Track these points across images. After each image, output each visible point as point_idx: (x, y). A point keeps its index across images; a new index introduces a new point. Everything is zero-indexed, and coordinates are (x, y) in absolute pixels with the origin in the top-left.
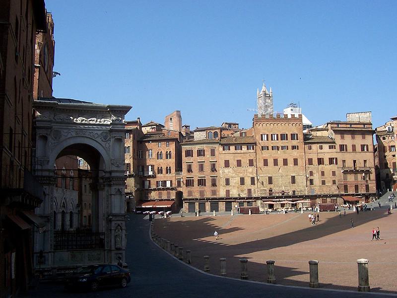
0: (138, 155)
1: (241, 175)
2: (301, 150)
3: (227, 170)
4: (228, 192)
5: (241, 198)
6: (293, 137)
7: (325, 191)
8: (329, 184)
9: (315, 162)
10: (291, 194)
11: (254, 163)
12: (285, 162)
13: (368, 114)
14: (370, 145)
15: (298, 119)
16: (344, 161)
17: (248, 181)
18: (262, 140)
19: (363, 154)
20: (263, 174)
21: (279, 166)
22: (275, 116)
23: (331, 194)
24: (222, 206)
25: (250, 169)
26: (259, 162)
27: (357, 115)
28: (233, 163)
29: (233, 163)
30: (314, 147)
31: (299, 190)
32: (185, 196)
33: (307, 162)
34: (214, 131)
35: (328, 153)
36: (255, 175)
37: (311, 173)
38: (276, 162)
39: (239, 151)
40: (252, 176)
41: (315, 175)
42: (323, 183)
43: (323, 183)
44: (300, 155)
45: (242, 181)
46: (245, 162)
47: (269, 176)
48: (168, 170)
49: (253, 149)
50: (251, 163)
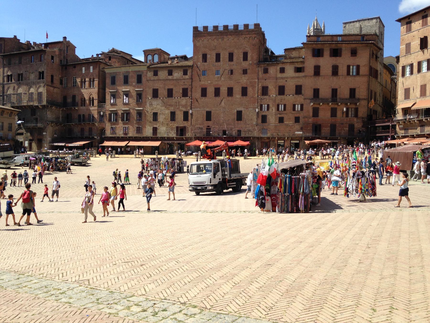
0: (61, 83)
1: (172, 109)
4: (155, 130)
7: (283, 131)
8: (289, 121)
10: (234, 133)
11: (189, 93)
12: (230, 92)
13: (374, 21)
14: (364, 66)
16: (316, 92)
19: (349, 79)
20: (200, 108)
22: (221, 29)
23: (291, 135)
25: (184, 101)
27: (357, 25)
28: (163, 92)
29: (163, 92)
30: (273, 70)
31: (246, 130)
32: (108, 133)
33: (260, 91)
35: (292, 78)
36: (189, 108)
38: (217, 92)
39: (170, 77)
40: (184, 110)
41: (270, 110)
42: (281, 120)
43: (281, 120)
44: (251, 82)
45: (173, 115)
46: (178, 91)
47: (208, 110)
48: (92, 100)
50: (185, 93)
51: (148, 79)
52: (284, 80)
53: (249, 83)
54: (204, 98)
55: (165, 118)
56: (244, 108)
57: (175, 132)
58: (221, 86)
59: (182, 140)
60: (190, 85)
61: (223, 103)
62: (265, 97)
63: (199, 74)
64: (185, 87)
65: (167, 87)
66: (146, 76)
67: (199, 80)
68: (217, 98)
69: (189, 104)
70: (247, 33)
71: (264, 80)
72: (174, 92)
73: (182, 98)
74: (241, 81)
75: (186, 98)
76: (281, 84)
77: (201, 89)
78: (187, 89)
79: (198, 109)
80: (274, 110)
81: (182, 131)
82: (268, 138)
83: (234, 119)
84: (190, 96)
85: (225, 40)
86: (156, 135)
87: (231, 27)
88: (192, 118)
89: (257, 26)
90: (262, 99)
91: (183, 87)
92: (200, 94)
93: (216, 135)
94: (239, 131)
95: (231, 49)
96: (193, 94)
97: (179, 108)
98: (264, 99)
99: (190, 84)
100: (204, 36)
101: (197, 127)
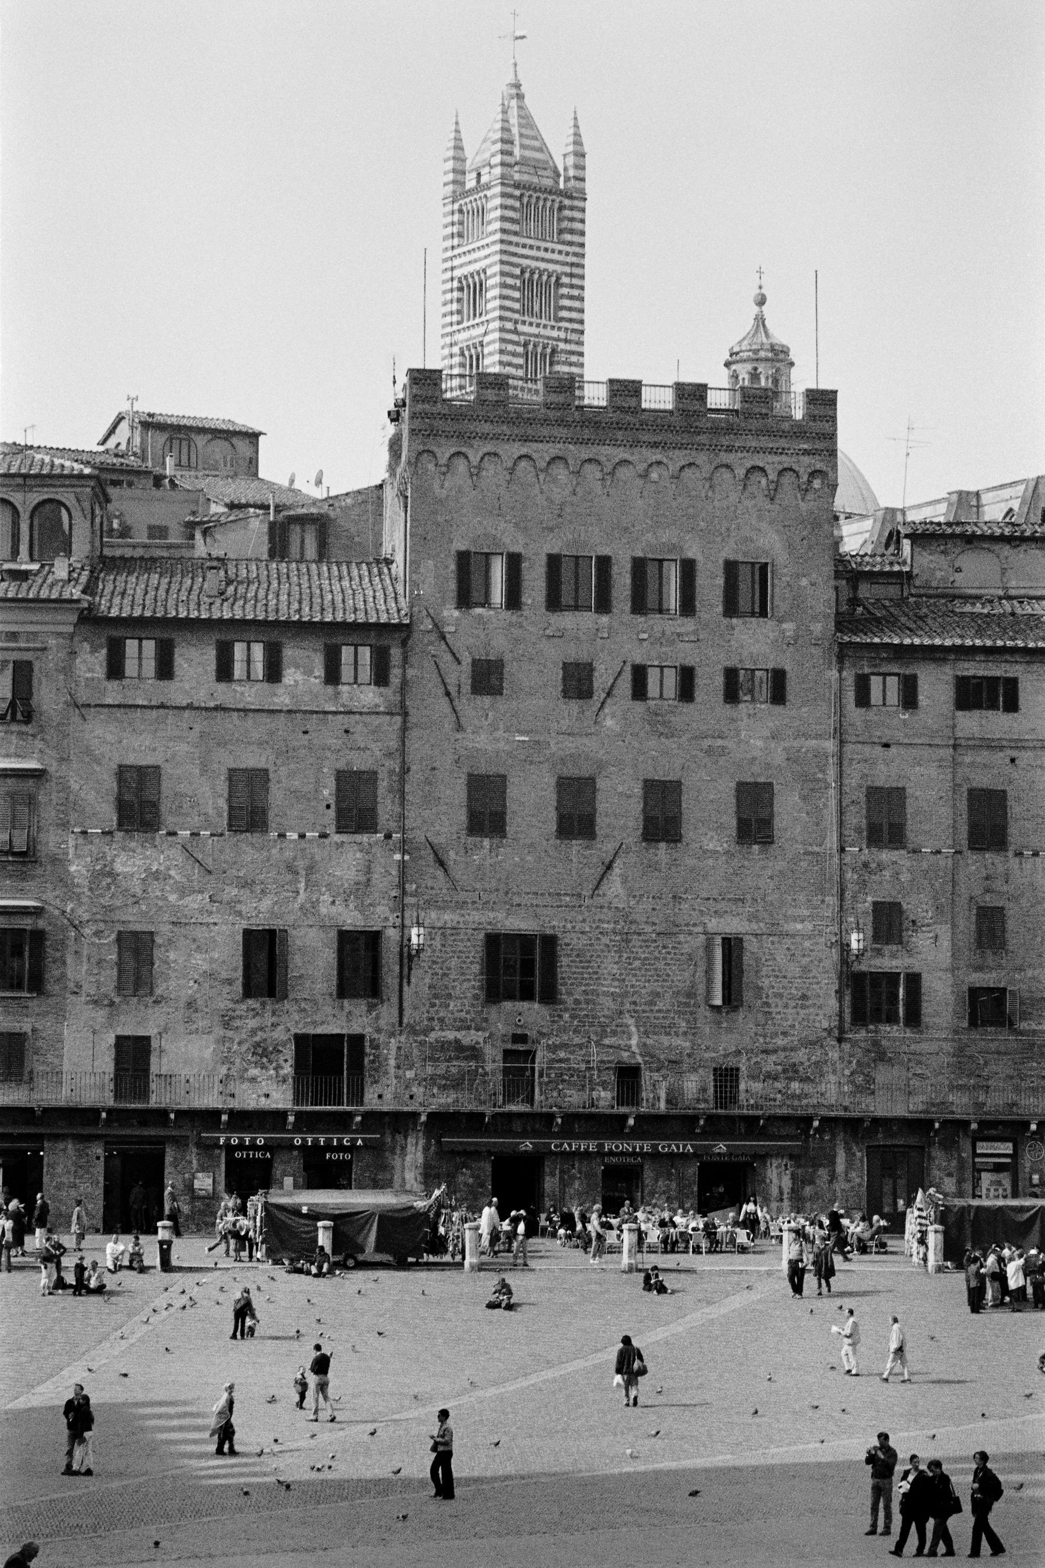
1: (261, 911)
2: (811, 711)
3: (132, 861)
4: (133, 1056)
5: (243, 1119)
6: (748, 589)
9: (935, 815)
11: (386, 809)
15: (798, 431)
17: (313, 960)
18: (464, 600)
21: (605, 847)
24: (74, 1177)
25: (346, 859)
26: (428, 800)
33: (856, 818)
34: (35, 497)
37: (889, 924)
40: (352, 919)
41: (921, 940)
49: (381, 678)
50: (355, 808)
51: (83, 697)
52: (1001, 758)
53: (779, 757)
54: (486, 842)
55: (211, 975)
56: (753, 917)
57: (288, 1069)
58: (601, 765)
59: (342, 1122)
60: (389, 755)
61: (614, 887)
62: (886, 856)
63: (451, 680)
64: (360, 763)
65: (225, 760)
66: (67, 670)
67: (448, 725)
68: (576, 846)
69: (384, 881)
70: (765, 442)
71: (879, 748)
72: (276, 796)
73: (337, 838)
74: (729, 744)
75: (364, 838)
76: (983, 780)
77: (463, 780)
78: (371, 777)
79: (449, 917)
80: (945, 943)
81: (327, 1063)
82: (918, 1126)
83: (691, 995)
84: (393, 825)
85: (623, 473)
86: (144, 1093)
87: (658, 399)
88: (404, 977)
89: (823, 401)
90: (866, 865)
91: (341, 765)
92: (462, 816)
93: (574, 1099)
94: (726, 1078)
95: (667, 536)
96: (411, 813)
97: (315, 904)
98: (881, 867)
99: (394, 744)
100: (485, 437)
101: (443, 1046)
